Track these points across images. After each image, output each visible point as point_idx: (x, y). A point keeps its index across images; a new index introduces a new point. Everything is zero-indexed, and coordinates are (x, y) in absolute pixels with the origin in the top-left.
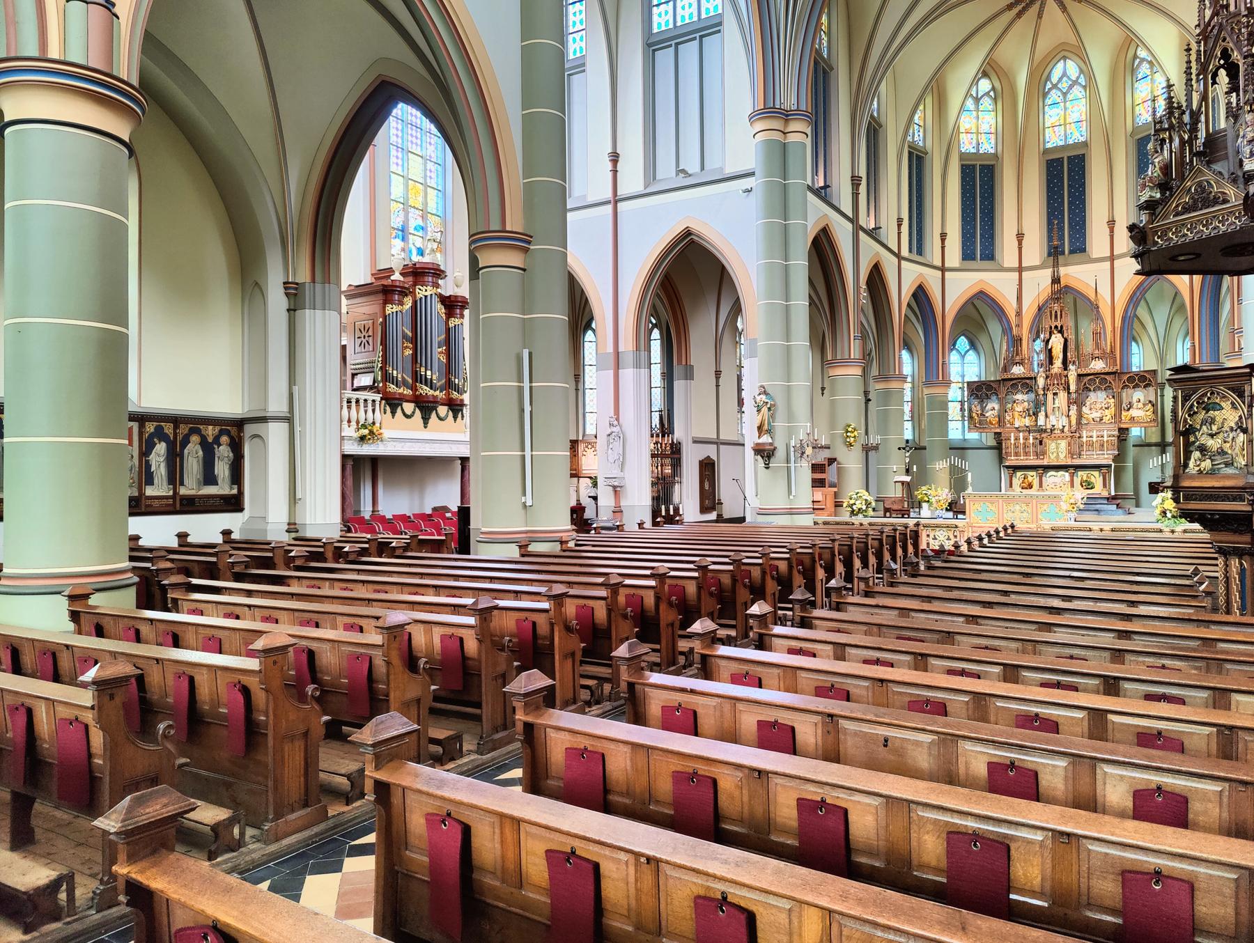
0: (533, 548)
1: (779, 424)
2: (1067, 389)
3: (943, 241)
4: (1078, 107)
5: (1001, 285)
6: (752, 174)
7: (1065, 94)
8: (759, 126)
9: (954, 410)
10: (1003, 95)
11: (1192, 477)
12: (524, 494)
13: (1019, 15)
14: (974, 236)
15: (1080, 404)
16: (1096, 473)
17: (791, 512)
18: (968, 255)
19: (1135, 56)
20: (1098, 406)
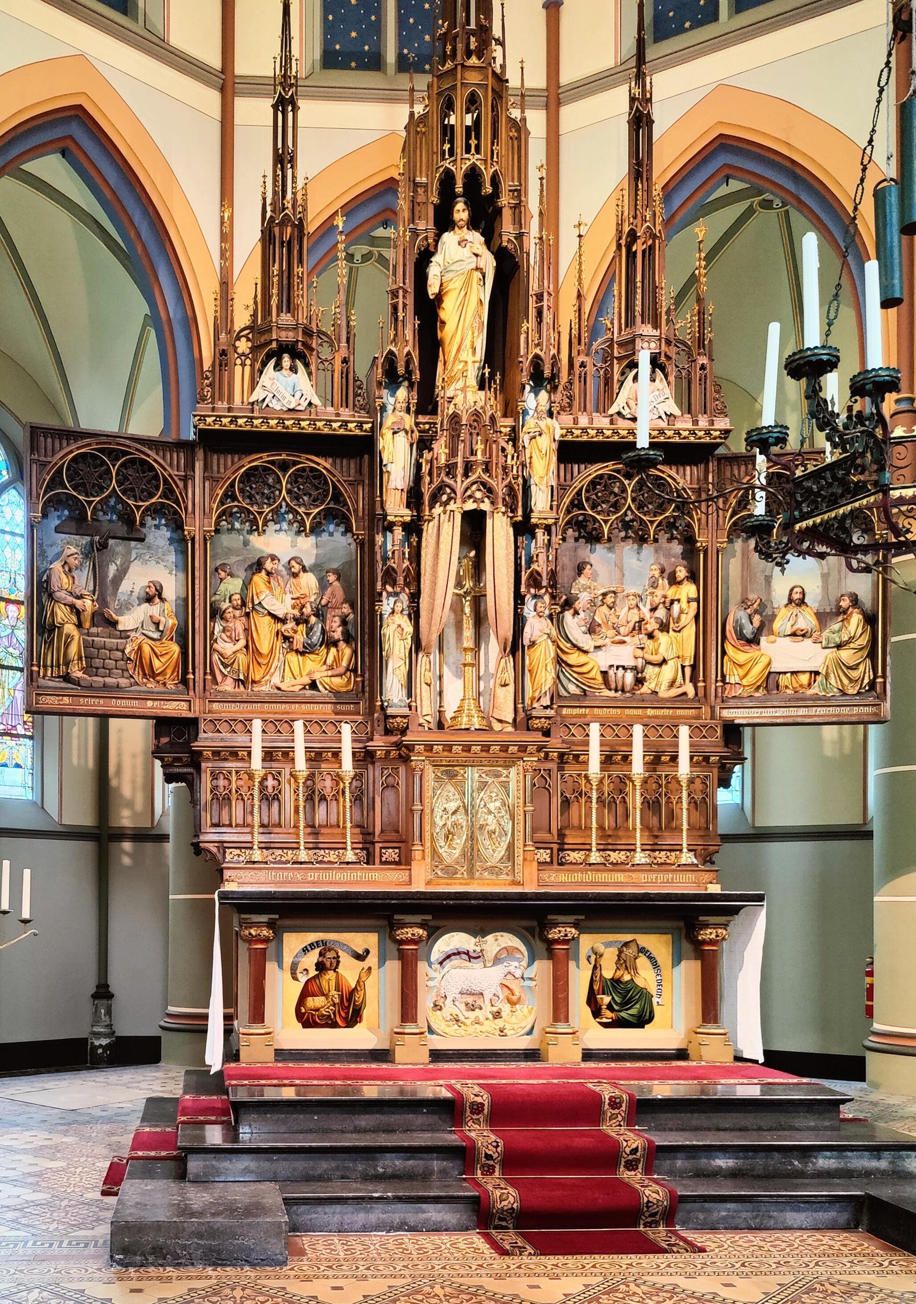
2: (518, 497)
16: (658, 944)
20: (626, 615)
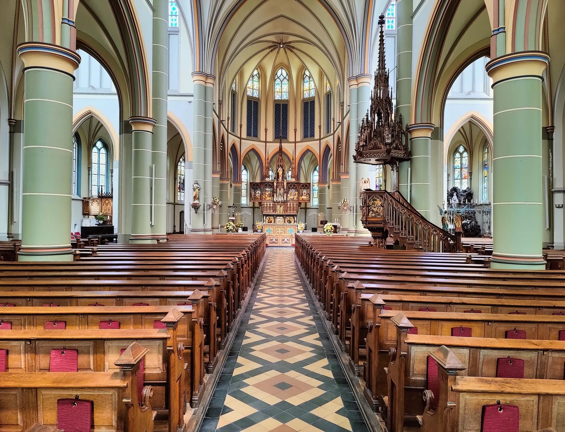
0: (161, 241)
1: (202, 196)
3: (241, 127)
4: (286, 87)
5: (260, 147)
6: (192, 96)
7: (282, 82)
8: (197, 78)
9: (244, 192)
10: (262, 76)
11: (370, 218)
12: (151, 221)
13: (272, 51)
14: (251, 127)
15: (287, 193)
17: (205, 230)
18: (249, 134)
19: (304, 74)
